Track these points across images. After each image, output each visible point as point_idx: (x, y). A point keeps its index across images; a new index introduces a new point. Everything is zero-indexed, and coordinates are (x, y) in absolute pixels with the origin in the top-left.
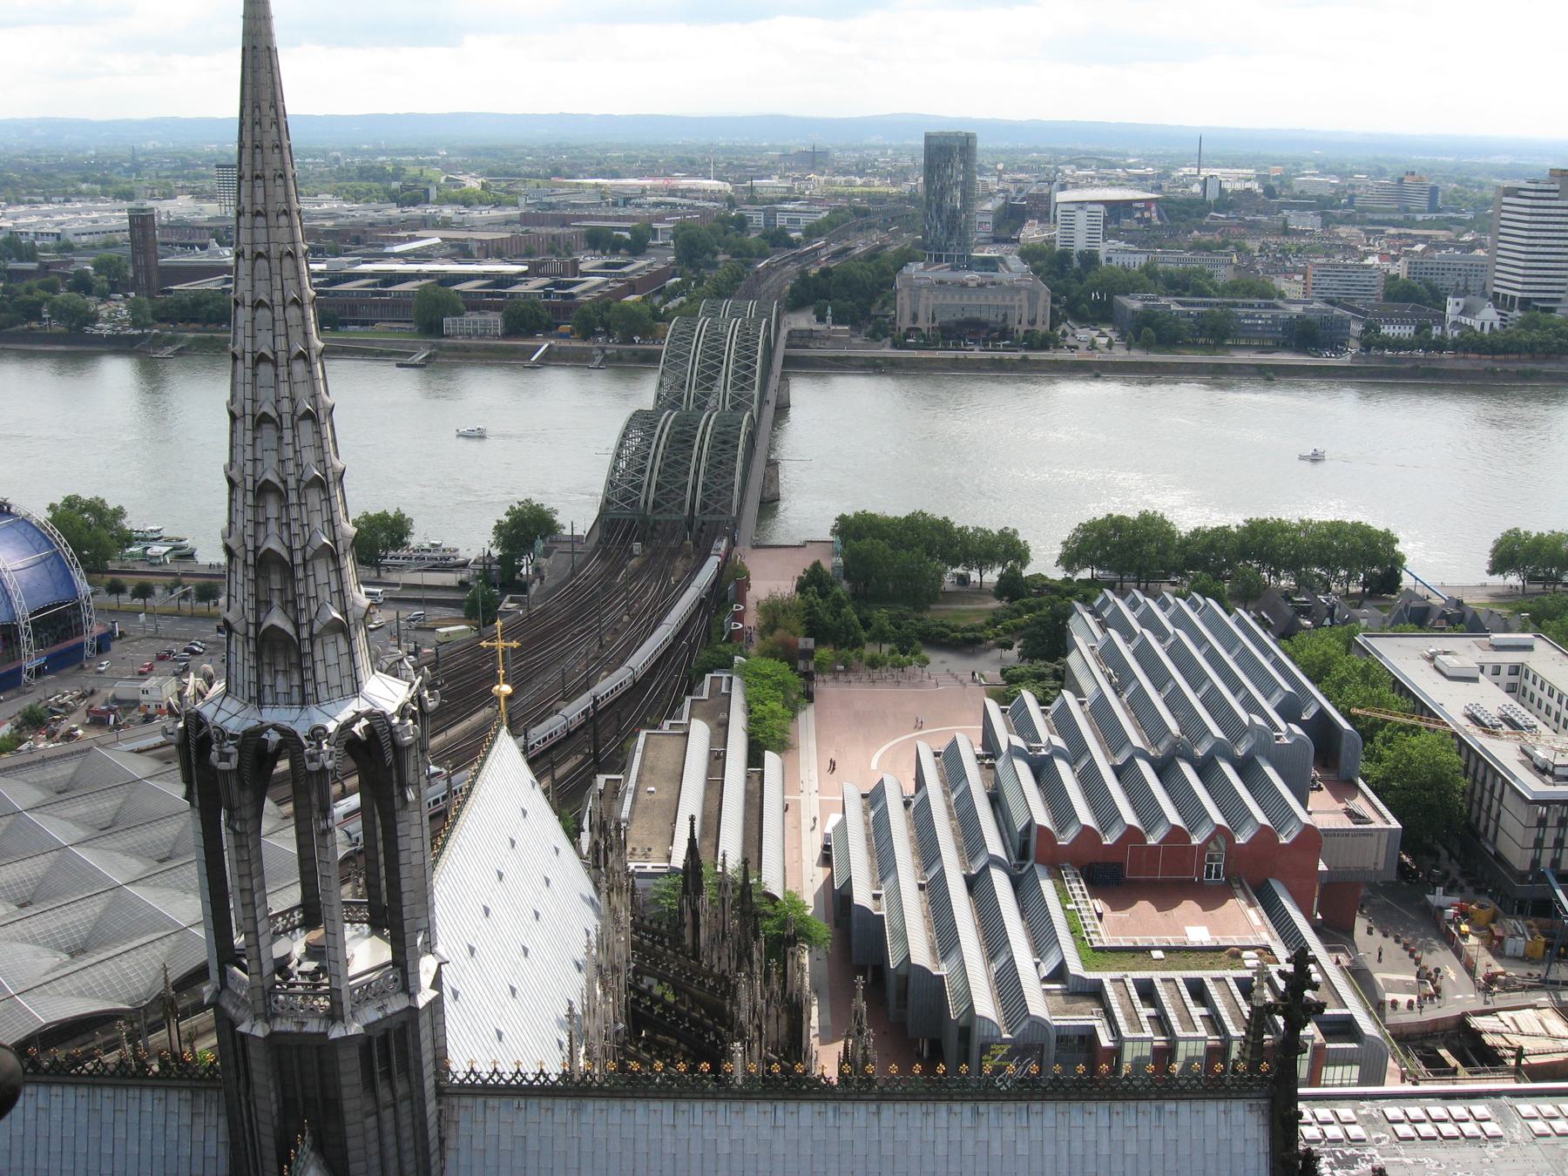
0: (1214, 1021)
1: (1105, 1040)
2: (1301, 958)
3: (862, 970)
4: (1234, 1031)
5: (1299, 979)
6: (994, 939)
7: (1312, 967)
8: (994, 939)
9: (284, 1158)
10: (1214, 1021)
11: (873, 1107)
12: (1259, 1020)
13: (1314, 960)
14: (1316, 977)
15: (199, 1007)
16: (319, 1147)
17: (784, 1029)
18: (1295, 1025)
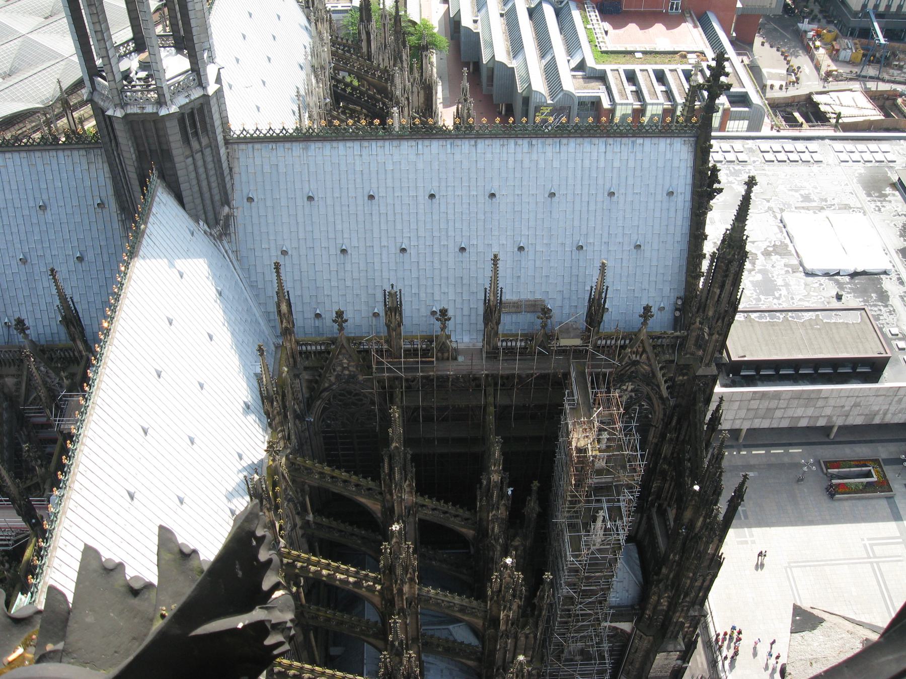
0: (669, 94)
1: (606, 104)
2: (721, 58)
3: (467, 64)
4: (680, 100)
5: (718, 70)
6: (544, 46)
7: (726, 64)
8: (544, 46)
9: (143, 183)
10: (669, 94)
11: (473, 142)
12: (694, 92)
13: (728, 59)
14: (728, 69)
15: (82, 104)
16: (162, 176)
17: (422, 100)
18: (713, 97)
